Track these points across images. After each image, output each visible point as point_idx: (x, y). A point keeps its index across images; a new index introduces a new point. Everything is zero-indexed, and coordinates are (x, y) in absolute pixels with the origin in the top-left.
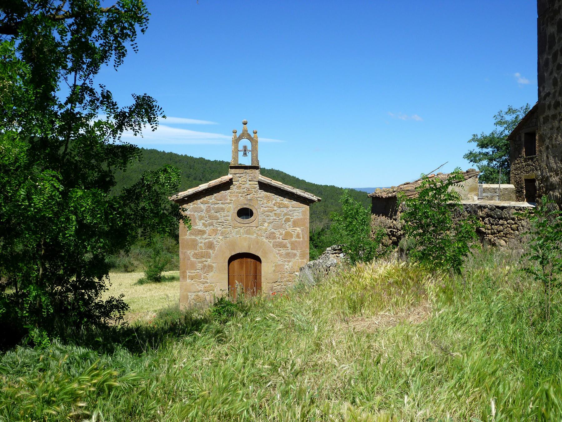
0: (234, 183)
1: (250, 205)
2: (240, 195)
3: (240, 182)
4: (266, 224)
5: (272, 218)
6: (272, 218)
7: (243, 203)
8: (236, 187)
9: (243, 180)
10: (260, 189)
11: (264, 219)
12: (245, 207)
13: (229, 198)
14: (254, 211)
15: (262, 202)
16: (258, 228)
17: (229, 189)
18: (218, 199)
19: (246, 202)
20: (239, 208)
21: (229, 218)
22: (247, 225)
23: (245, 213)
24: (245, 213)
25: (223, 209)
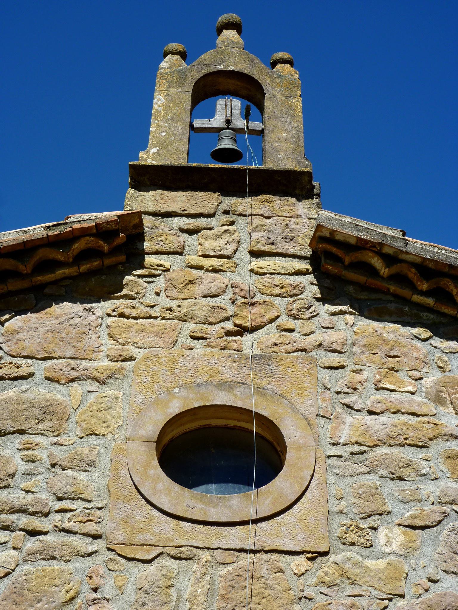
0: (149, 260)
1: (260, 391)
2: (189, 327)
3: (194, 259)
4: (390, 538)
5: (431, 489)
6: (431, 489)
7: (202, 377)
8: (160, 283)
9: (210, 245)
10: (325, 298)
11: (374, 493)
12: (221, 398)
13: (108, 344)
14: (291, 431)
15: (346, 377)
16: (325, 568)
17: (110, 289)
18: (30, 347)
19: (229, 373)
20: (175, 408)
21: (91, 481)
22: (235, 537)
23: (218, 450)
24: (218, 450)
25: (51, 417)
